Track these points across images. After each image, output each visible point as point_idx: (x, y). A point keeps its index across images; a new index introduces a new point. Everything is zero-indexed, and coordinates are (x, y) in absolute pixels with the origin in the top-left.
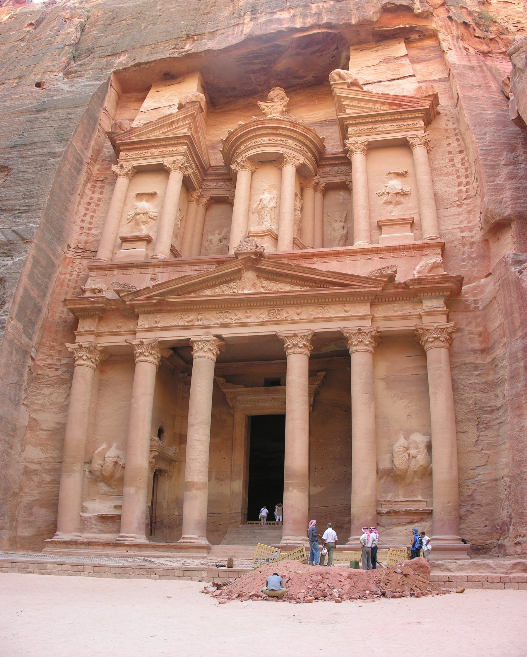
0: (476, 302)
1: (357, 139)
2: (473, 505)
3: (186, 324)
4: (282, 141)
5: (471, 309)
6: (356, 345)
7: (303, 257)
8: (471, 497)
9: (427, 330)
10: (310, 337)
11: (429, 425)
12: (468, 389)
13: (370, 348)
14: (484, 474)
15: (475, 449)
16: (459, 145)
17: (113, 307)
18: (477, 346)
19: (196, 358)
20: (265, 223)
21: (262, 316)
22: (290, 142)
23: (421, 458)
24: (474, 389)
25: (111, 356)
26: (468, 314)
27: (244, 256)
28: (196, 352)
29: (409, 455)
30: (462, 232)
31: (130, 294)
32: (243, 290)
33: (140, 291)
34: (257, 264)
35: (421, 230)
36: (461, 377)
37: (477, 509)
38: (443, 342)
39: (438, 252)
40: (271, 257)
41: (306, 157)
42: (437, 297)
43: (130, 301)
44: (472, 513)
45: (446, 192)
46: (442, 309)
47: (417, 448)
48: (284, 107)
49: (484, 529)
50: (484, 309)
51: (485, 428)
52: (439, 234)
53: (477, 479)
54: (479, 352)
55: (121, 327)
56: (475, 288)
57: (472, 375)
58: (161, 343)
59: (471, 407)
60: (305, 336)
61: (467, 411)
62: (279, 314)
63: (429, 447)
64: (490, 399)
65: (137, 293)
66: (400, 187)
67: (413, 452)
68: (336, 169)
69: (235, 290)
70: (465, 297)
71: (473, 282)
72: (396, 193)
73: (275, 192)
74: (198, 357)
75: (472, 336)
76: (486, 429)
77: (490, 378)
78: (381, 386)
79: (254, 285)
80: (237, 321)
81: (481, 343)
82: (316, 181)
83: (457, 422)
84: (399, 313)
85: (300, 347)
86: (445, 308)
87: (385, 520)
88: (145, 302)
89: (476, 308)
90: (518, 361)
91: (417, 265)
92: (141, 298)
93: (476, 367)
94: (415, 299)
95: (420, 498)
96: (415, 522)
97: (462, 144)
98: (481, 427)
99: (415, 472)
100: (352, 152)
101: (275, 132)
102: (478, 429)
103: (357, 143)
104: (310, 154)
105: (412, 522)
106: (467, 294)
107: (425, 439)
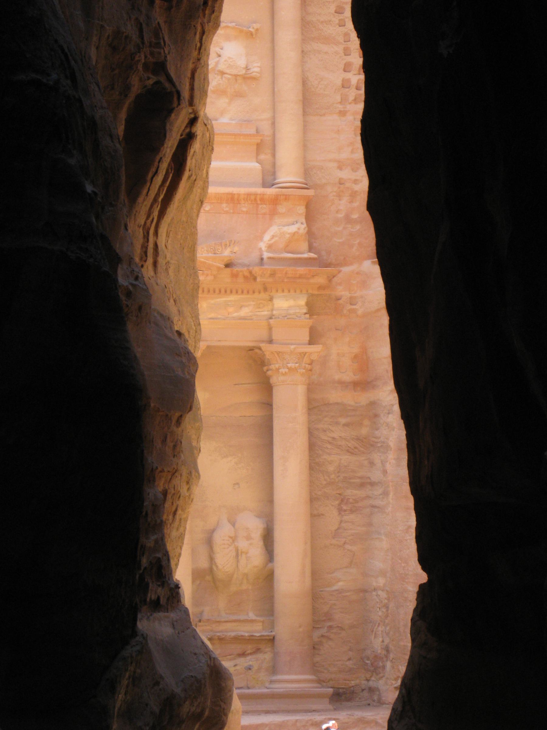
2: (330, 627)
5: (345, 312)
8: (328, 617)
12: (329, 446)
23: (255, 554)
24: (339, 447)
30: (340, 168)
36: (320, 426)
44: (329, 638)
47: (248, 538)
49: (347, 663)
57: (337, 423)
59: (333, 476)
61: (325, 482)
63: (268, 538)
66: (242, 62)
67: (242, 544)
71: (351, 264)
76: (352, 511)
91: (264, 232)
95: (252, 616)
96: (248, 654)
98: (345, 508)
99: (246, 575)
102: (340, 511)
105: (243, 654)
106: (340, 284)
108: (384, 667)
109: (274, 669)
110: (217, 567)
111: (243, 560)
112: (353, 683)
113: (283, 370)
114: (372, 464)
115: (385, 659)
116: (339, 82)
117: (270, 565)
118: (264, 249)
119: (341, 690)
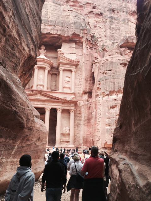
1: (61, 68)
7: (49, 92)
8: (76, 139)
11: (70, 126)
22: (47, 65)
40: (43, 91)
41: (50, 68)
52: (75, 91)
63: (69, 130)
67: (66, 130)
68: (55, 70)
78: (62, 118)
79: (40, 97)
87: (61, 142)
93: (78, 116)
99: (67, 134)
107: (69, 128)
109: (69, 145)
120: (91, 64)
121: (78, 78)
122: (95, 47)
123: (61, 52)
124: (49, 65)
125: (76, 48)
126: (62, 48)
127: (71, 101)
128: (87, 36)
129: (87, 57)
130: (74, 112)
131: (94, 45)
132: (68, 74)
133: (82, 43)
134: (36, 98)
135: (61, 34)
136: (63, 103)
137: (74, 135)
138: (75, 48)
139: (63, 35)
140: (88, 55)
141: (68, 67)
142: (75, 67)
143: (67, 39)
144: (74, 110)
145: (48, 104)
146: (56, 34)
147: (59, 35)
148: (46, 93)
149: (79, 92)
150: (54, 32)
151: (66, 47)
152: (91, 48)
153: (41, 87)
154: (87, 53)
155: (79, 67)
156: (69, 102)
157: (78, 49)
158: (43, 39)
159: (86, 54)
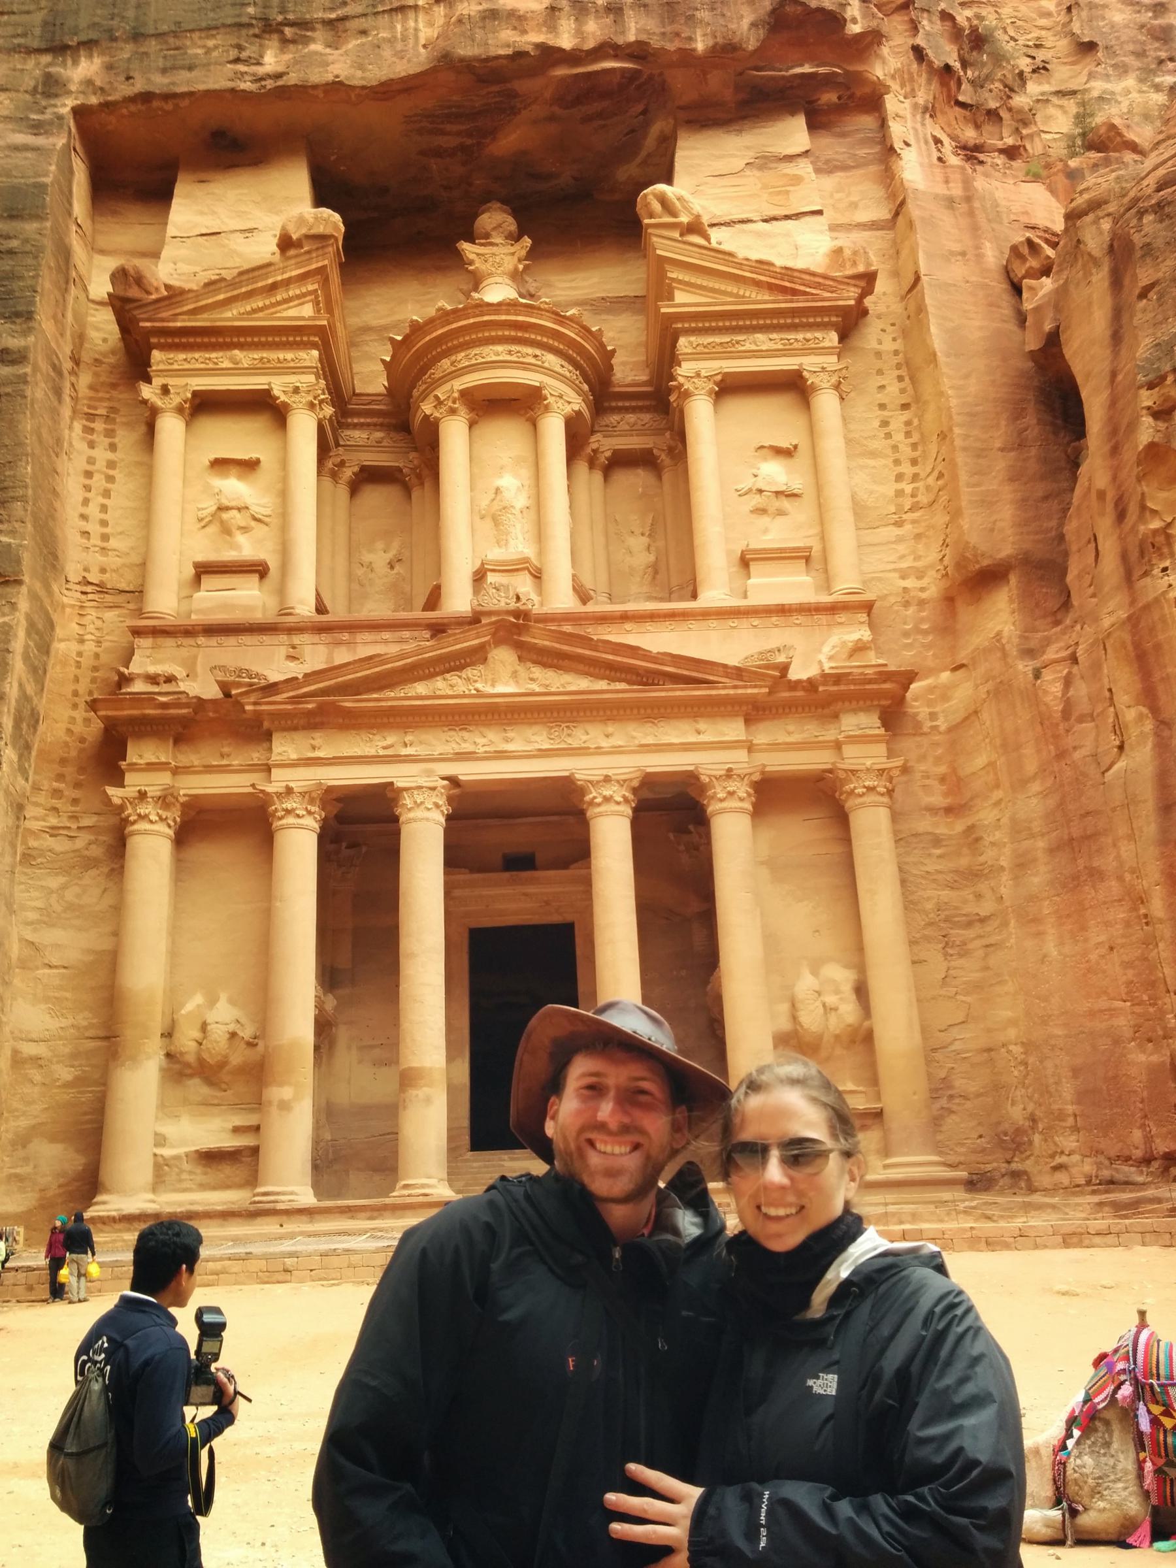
0: (933, 716)
1: (696, 368)
2: (951, 1097)
3: (381, 752)
4: (536, 356)
5: (925, 729)
6: (721, 800)
7: (603, 619)
8: (946, 1082)
9: (852, 771)
10: (636, 783)
11: (860, 948)
13: (748, 805)
14: (967, 1039)
15: (943, 992)
16: (903, 391)
17: (211, 714)
18: (937, 799)
19: (409, 821)
20: (512, 542)
21: (534, 738)
22: (552, 360)
23: (849, 1011)
25: (200, 811)
26: (918, 739)
27: (494, 619)
28: (410, 810)
29: (824, 1005)
30: (903, 578)
31: (254, 690)
32: (493, 686)
33: (275, 684)
34: (519, 634)
35: (826, 571)
36: (910, 859)
37: (959, 1104)
38: (882, 795)
39: (862, 620)
41: (580, 391)
42: (866, 710)
43: (255, 704)
45: (871, 493)
46: (877, 732)
47: (837, 992)
48: (520, 260)
50: (950, 730)
51: (959, 954)
52: (864, 582)
53: (953, 1048)
54: (942, 812)
55: (228, 756)
56: (931, 689)
57: (929, 855)
58: (330, 790)
59: (932, 915)
60: (625, 781)
62: (569, 735)
63: (861, 991)
64: (965, 902)
65: (272, 688)
67: (831, 999)
68: (631, 418)
69: (479, 686)
70: (912, 707)
71: (927, 678)
72: (777, 493)
73: (526, 473)
74: (409, 821)
75: (927, 782)
76: (961, 956)
77: (964, 862)
80: (487, 749)
81: (946, 795)
82: (594, 446)
83: (912, 943)
84: (795, 738)
85: (618, 803)
86: (882, 731)
88: (289, 707)
89: (935, 728)
90: (1032, 836)
91: (822, 644)
92: (278, 698)
93: (937, 841)
94: (826, 711)
97: (910, 389)
98: (950, 951)
100: (687, 395)
101: (520, 334)
102: (946, 955)
103: (698, 375)
104: (586, 387)
106: (916, 700)
108: (1031, 1143)
110: (802, 1027)
111: (833, 1020)
112: (989, 1167)
113: (860, 791)
114: (979, 896)
115: (1030, 1132)
116: (892, 493)
117: (866, 1024)
118: (824, 660)
119: (975, 1177)
120: (1000, 287)
121: (873, 454)
122: (1010, 141)
123: (674, 214)
124: (576, 366)
125: (826, 168)
126: (676, 180)
127: (838, 679)
128: (914, 27)
129: (946, 220)
130: (890, 792)
131: (993, 115)
132: (768, 419)
133: (873, 102)
134: (480, 694)
135: (656, 43)
136: (755, 712)
137: (918, 1036)
138: (804, 168)
139: (671, 46)
140: (950, 202)
141: (763, 353)
142: (832, 338)
143: (717, 83)
144: (881, 772)
145: (605, 743)
146: (605, 49)
147: (639, 52)
148: (568, 628)
149: (909, 583)
150: (579, 33)
151: (720, 166)
152: (972, 153)
153: (524, 585)
154: (941, 189)
155: (877, 336)
156: (822, 698)
157: (844, 168)
158: (493, 133)
159: (936, 197)
